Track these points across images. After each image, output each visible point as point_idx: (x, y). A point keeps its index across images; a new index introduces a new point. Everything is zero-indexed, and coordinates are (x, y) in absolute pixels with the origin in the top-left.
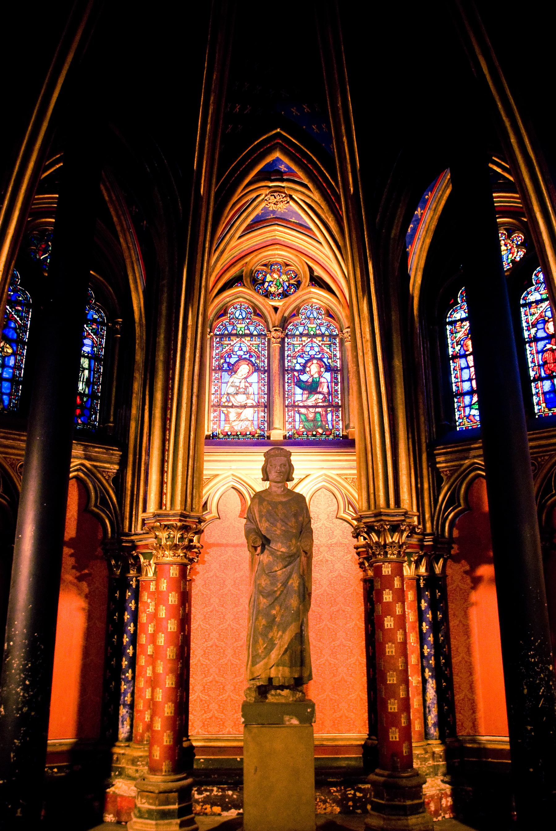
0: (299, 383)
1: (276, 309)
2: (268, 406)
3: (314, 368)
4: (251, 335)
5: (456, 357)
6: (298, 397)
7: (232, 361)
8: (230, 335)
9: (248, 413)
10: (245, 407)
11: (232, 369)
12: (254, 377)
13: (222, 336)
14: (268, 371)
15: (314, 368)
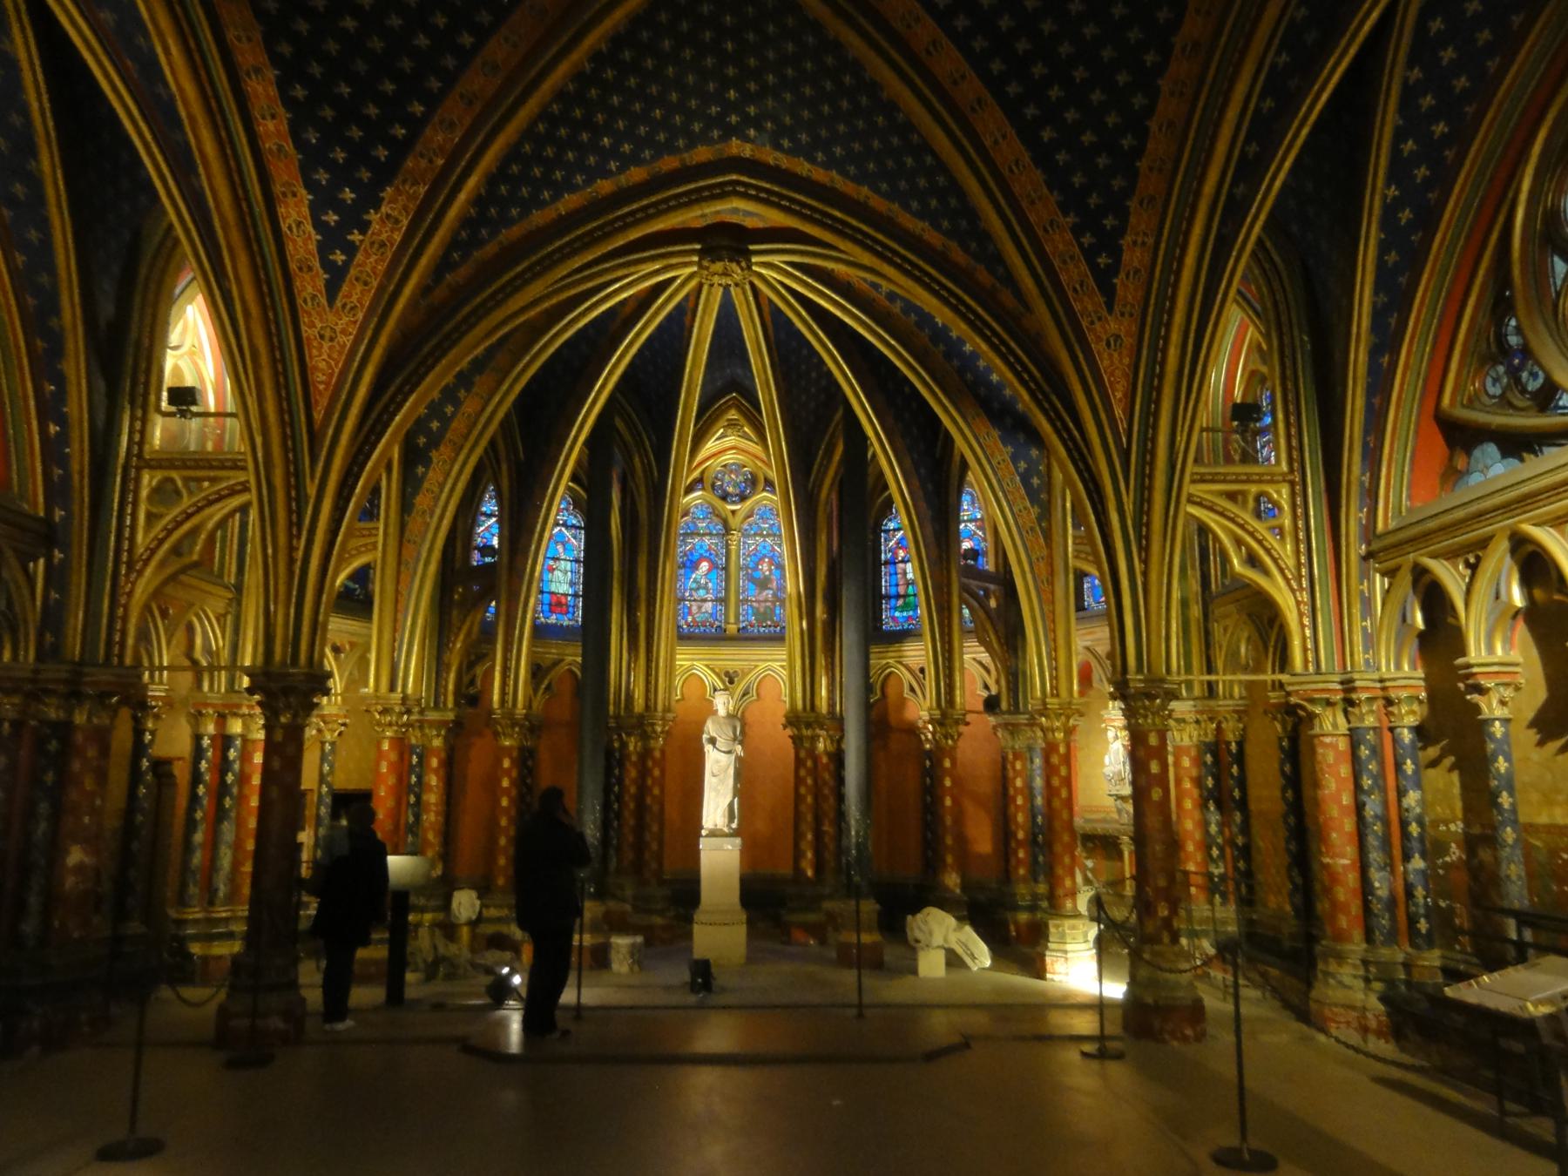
0: (752, 579)
1: (733, 512)
2: (723, 601)
3: (765, 567)
4: (710, 534)
5: (887, 563)
6: (751, 593)
7: (696, 556)
8: (693, 534)
9: (708, 606)
10: (705, 600)
11: (695, 566)
12: (713, 575)
13: (686, 535)
14: (726, 569)
15: (765, 567)
